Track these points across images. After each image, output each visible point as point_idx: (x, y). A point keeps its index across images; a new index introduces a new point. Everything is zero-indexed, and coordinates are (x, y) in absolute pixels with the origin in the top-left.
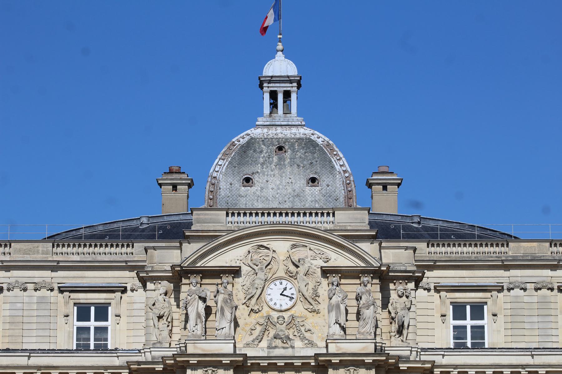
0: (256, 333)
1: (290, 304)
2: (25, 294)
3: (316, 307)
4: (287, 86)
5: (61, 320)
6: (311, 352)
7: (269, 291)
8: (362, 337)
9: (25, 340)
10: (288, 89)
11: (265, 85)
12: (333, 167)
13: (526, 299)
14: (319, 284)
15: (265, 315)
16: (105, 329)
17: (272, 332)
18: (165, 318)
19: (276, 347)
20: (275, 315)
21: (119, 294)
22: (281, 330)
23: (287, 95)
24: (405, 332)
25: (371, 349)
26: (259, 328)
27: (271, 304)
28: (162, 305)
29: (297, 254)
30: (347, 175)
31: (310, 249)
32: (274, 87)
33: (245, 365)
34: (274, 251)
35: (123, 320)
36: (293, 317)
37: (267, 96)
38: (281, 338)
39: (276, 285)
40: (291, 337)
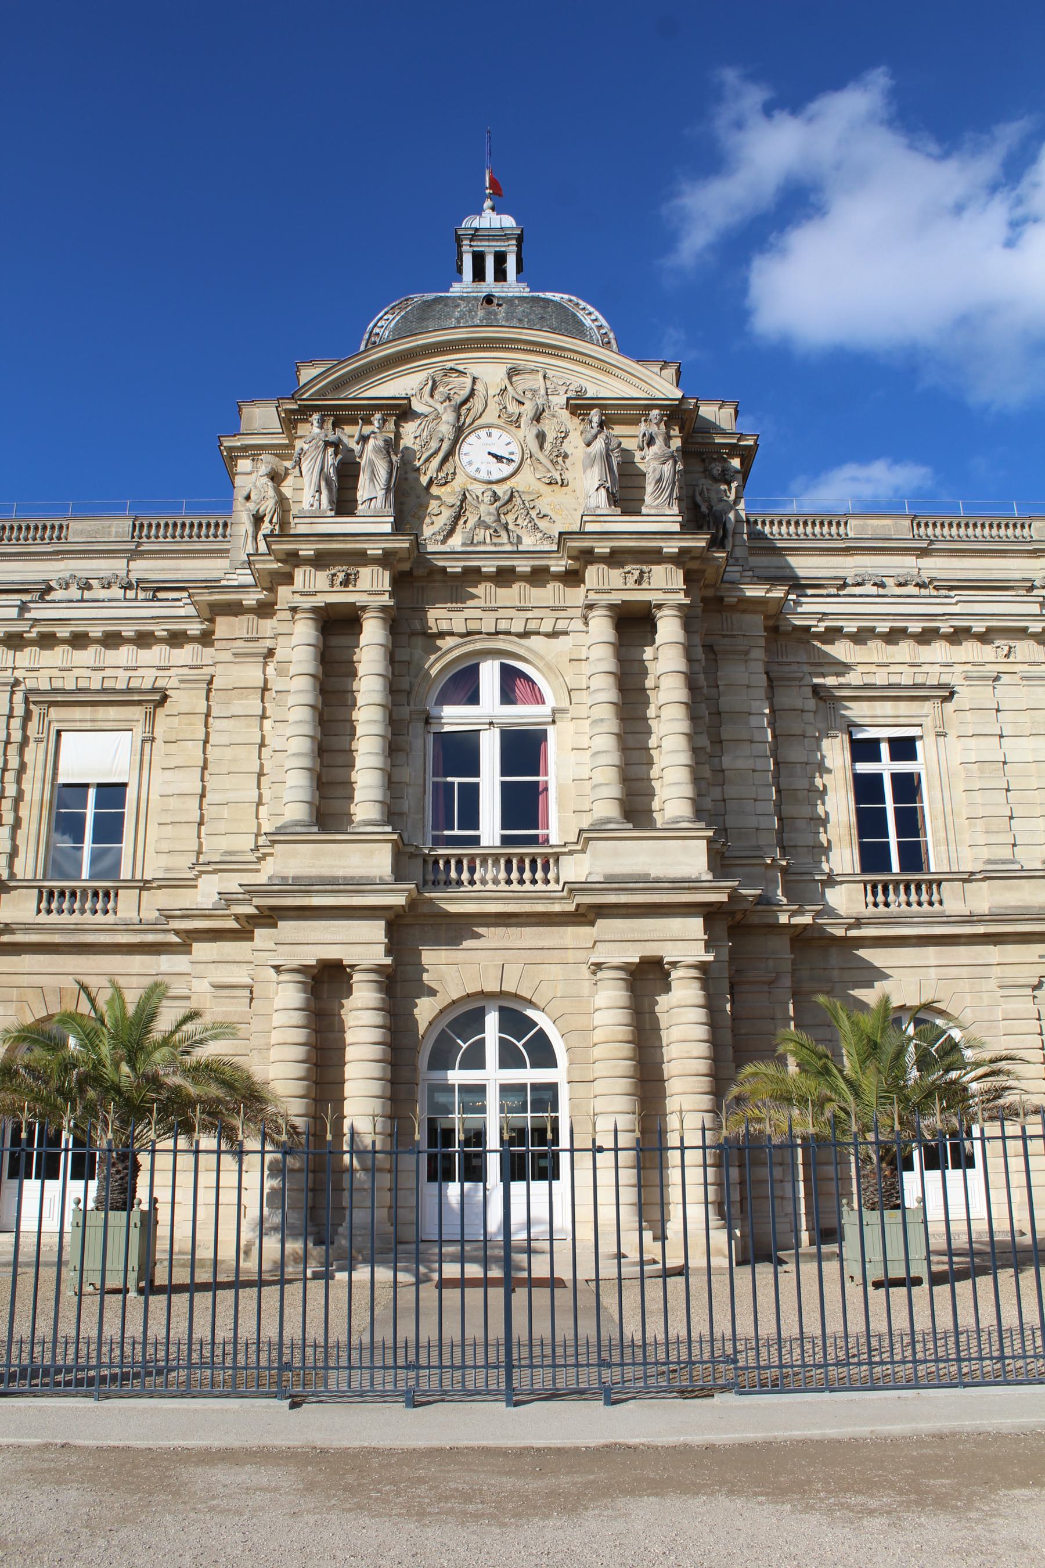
1: (507, 469)
4: (500, 246)
7: (465, 448)
8: (653, 512)
10: (503, 249)
11: (465, 242)
14: (563, 435)
15: (458, 489)
18: (267, 519)
20: (477, 489)
22: (489, 514)
23: (500, 259)
27: (471, 470)
31: (544, 377)
32: (480, 246)
33: (415, 573)
37: (468, 261)
38: (488, 527)
39: (479, 438)
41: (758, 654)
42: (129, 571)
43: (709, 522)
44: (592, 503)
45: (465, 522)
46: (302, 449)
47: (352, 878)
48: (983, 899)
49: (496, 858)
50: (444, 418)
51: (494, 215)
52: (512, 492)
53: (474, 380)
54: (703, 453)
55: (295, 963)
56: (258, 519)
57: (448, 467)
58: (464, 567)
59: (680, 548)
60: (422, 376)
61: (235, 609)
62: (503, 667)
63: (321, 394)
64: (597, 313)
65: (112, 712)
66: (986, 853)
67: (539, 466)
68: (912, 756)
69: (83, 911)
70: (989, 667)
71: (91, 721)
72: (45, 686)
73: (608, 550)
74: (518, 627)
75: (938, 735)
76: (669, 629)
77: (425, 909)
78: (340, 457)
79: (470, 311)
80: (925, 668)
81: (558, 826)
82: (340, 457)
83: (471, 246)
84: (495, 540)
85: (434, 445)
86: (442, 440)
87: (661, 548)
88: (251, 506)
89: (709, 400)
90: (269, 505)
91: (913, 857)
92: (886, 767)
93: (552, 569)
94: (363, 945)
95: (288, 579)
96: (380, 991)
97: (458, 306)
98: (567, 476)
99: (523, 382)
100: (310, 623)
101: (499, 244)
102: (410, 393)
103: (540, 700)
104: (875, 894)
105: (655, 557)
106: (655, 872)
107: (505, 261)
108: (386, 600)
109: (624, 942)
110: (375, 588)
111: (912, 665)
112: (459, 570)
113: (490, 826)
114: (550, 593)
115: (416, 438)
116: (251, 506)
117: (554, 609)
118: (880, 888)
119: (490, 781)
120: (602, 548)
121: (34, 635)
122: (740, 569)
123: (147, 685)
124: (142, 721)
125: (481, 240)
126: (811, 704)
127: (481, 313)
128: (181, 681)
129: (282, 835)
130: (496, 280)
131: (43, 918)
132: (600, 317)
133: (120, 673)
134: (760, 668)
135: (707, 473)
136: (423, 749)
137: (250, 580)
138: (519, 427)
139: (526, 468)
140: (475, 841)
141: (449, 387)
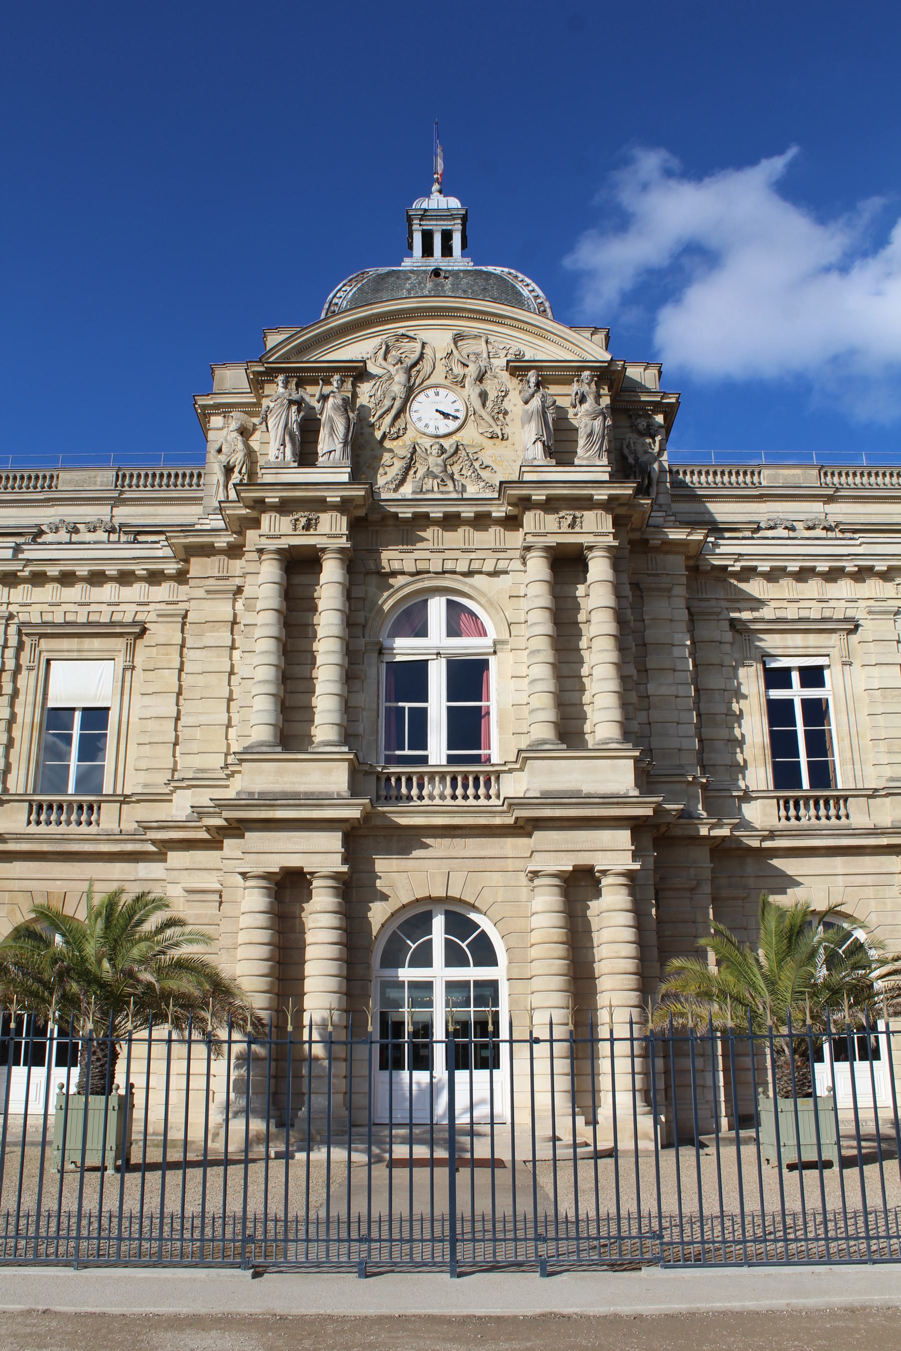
1: (453, 425)
4: (446, 225)
7: (415, 406)
8: (584, 463)
11: (415, 222)
14: (503, 394)
17: (422, 471)
18: (236, 470)
20: (426, 442)
22: (437, 465)
23: (447, 236)
27: (420, 426)
28: (233, 448)
30: (539, 301)
31: (487, 342)
32: (428, 225)
33: (370, 518)
38: (435, 477)
39: (428, 396)
41: (680, 591)
42: (112, 516)
43: (635, 472)
44: (530, 455)
45: (415, 473)
46: (268, 407)
47: (313, 793)
48: (886, 813)
49: (443, 776)
50: (396, 379)
51: (441, 198)
52: (457, 446)
53: (424, 345)
54: (629, 410)
55: (261, 870)
56: (228, 470)
57: (400, 423)
58: (414, 513)
59: (609, 495)
60: (377, 341)
61: (207, 551)
62: (449, 602)
63: (285, 358)
64: (533, 285)
65: (97, 643)
66: (888, 772)
67: (482, 422)
68: (820, 683)
69: (69, 823)
70: (890, 603)
71: (78, 651)
72: (36, 619)
73: (544, 498)
74: (462, 567)
75: (844, 664)
76: (599, 568)
77: (378, 822)
78: (302, 414)
79: (420, 283)
80: (832, 604)
81: (498, 747)
82: (302, 414)
83: (420, 225)
84: (442, 489)
85: (387, 403)
86: (394, 399)
87: (592, 495)
88: (223, 458)
89: (635, 363)
90: (238, 457)
91: (822, 775)
92: (797, 693)
93: (494, 514)
94: (322, 854)
96: (337, 896)
97: (409, 279)
98: (507, 430)
99: (468, 347)
100: (275, 563)
101: (445, 223)
102: (365, 356)
103: (483, 633)
104: (787, 809)
105: (588, 503)
106: (587, 788)
107: (451, 239)
108: (343, 542)
109: (558, 851)
110: (333, 532)
111: (820, 601)
112: (410, 515)
113: (437, 748)
114: (491, 536)
115: (371, 396)
116: (223, 458)
117: (495, 551)
118: (791, 803)
119: (437, 704)
120: (539, 495)
121: (27, 573)
122: (663, 514)
123: (128, 618)
124: (123, 651)
125: (430, 220)
126: (728, 636)
127: (429, 285)
128: (159, 616)
129: (249, 754)
130: (443, 255)
131: (33, 829)
132: (537, 288)
133: (104, 607)
134: (681, 603)
135: (634, 428)
136: (377, 677)
137: (221, 524)
138: (464, 387)
139: (470, 424)
140: (424, 760)
141: (401, 351)
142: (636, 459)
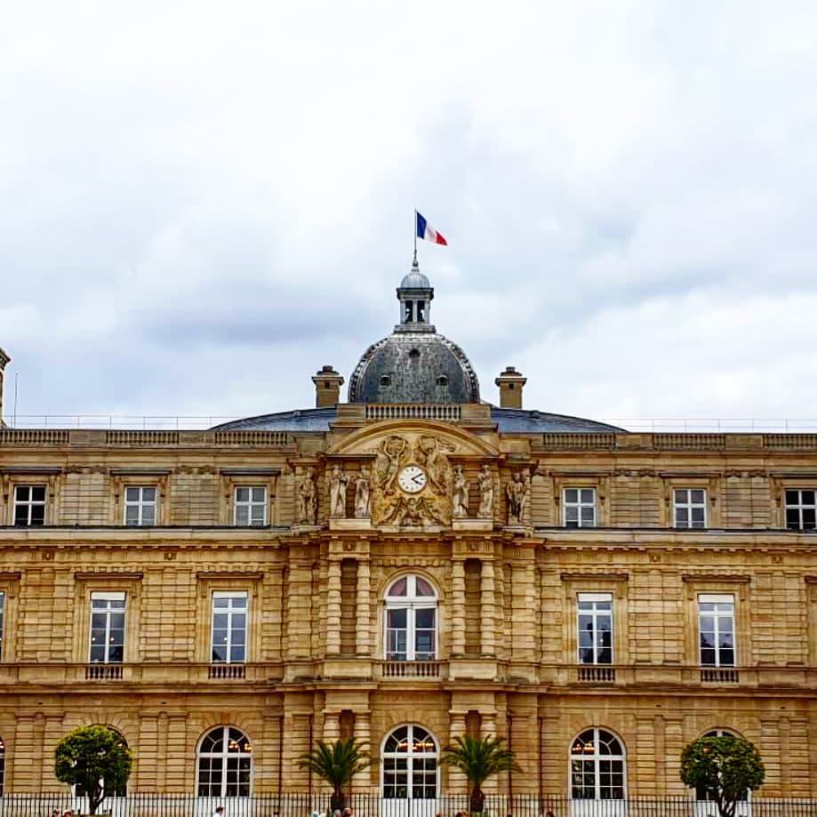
0: (390, 512)
1: (420, 487)
2: (191, 477)
3: (442, 491)
4: (421, 298)
5: (222, 500)
6: (437, 529)
9: (191, 517)
12: (460, 368)
13: (631, 485)
15: (398, 496)
16: (42, 507)
17: (404, 512)
19: (407, 525)
20: (407, 497)
21: (273, 478)
24: (521, 513)
25: (490, 527)
26: (392, 508)
27: (404, 487)
29: (429, 443)
31: (438, 440)
34: (407, 442)
35: (277, 499)
36: (422, 499)
38: (412, 517)
40: (421, 516)
49: (413, 665)
56: (307, 499)
62: (417, 578)
65: (238, 584)
74: (424, 563)
76: (488, 571)
80: (616, 566)
93: (439, 540)
95: (327, 542)
103: (433, 594)
106: (476, 677)
123: (255, 570)
126: (559, 583)
131: (212, 681)
133: (241, 564)
135: (513, 478)
136: (383, 616)
142: (513, 496)
